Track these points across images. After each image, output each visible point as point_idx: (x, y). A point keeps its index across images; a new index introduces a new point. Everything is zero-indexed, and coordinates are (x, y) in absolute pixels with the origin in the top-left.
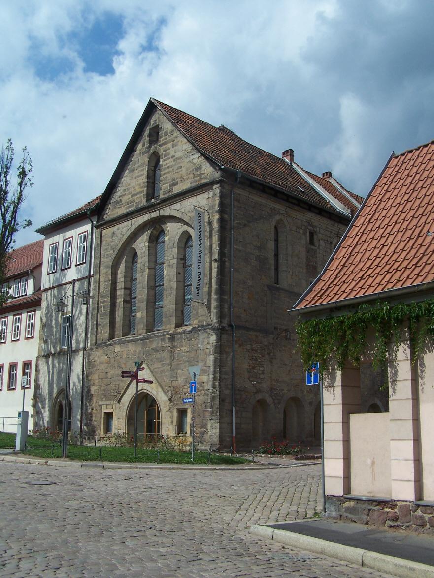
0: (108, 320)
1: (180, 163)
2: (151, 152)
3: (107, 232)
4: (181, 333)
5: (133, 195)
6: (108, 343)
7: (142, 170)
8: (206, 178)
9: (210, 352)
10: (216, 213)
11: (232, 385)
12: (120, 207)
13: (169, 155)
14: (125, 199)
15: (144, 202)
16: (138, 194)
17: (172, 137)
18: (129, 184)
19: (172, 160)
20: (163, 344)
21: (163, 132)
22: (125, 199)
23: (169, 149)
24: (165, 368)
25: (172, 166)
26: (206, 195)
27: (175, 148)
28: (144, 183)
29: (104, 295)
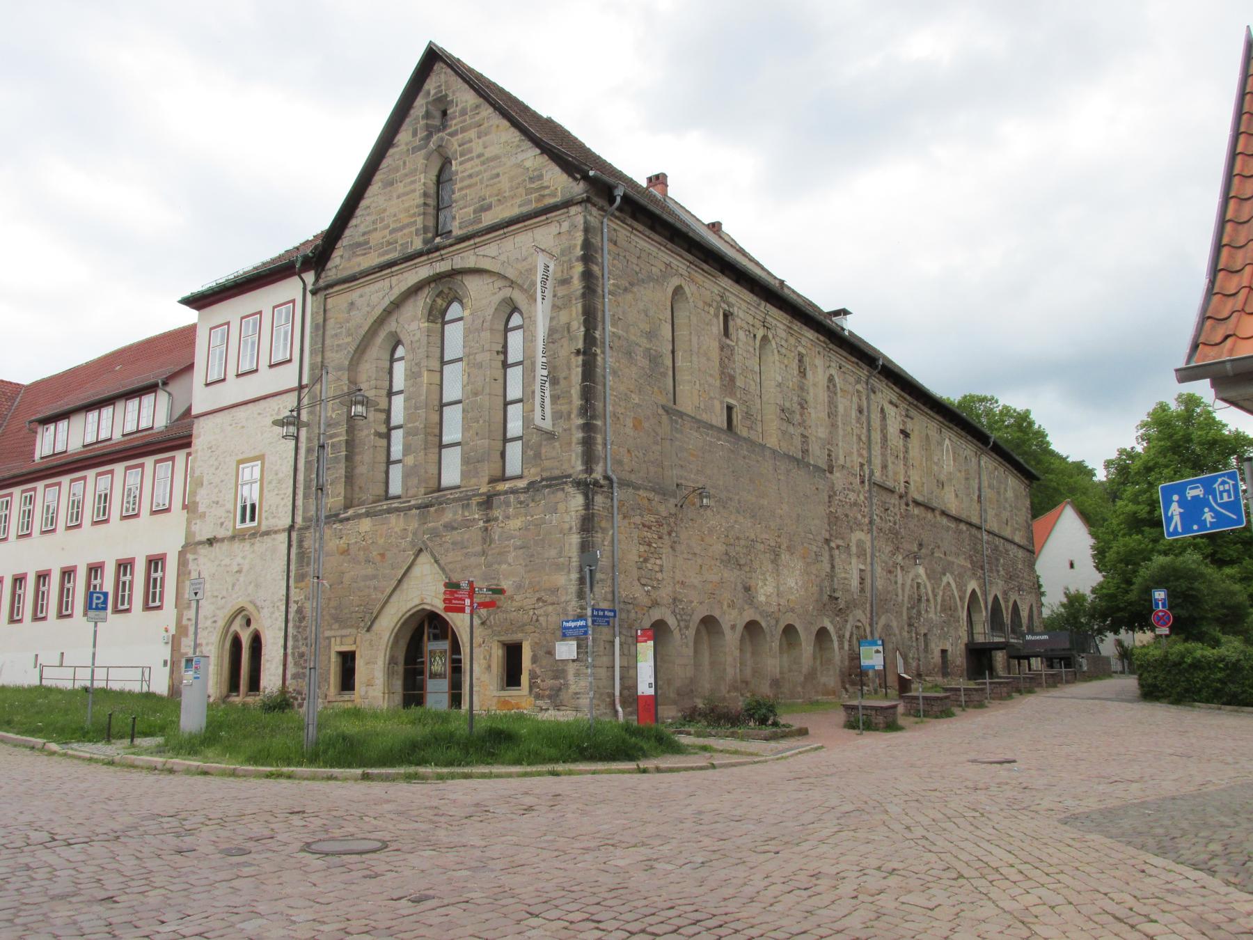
0: (343, 472)
1: (494, 168)
2: (432, 145)
3: (338, 302)
4: (506, 493)
6: (342, 516)
7: (413, 182)
8: (553, 195)
9: (571, 529)
10: (577, 260)
11: (613, 592)
12: (365, 254)
13: (470, 151)
14: (375, 238)
15: (418, 244)
16: (401, 229)
17: (477, 118)
18: (385, 210)
19: (477, 161)
20: (467, 514)
21: (458, 108)
22: (375, 238)
23: (470, 141)
24: (473, 560)
25: (478, 174)
26: (554, 229)
27: (484, 139)
28: (418, 206)
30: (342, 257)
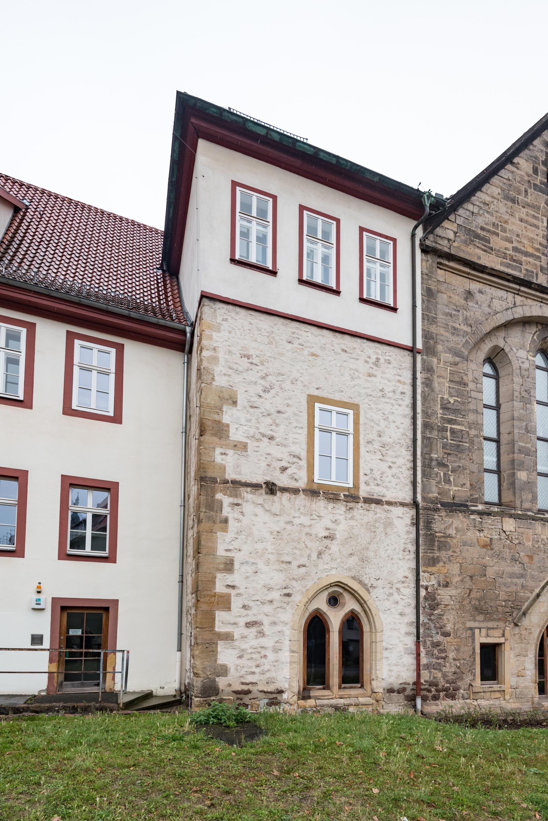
5: (515, 249)
14: (497, 242)
29: (449, 406)
30: (455, 233)
